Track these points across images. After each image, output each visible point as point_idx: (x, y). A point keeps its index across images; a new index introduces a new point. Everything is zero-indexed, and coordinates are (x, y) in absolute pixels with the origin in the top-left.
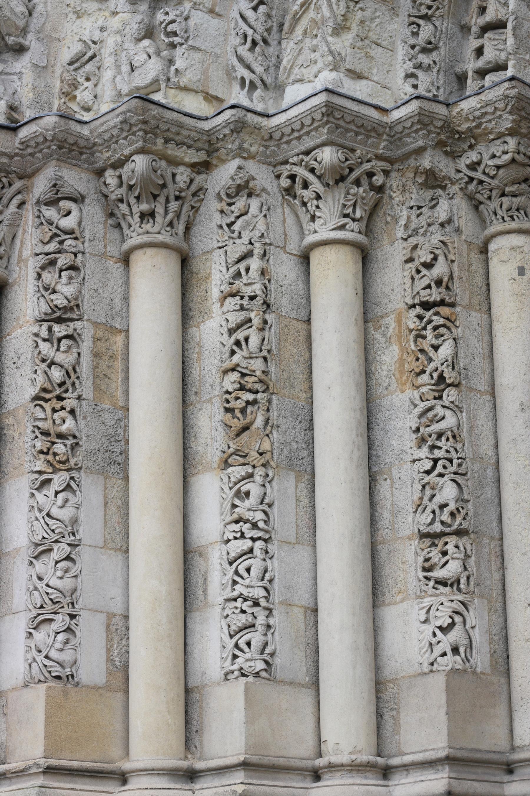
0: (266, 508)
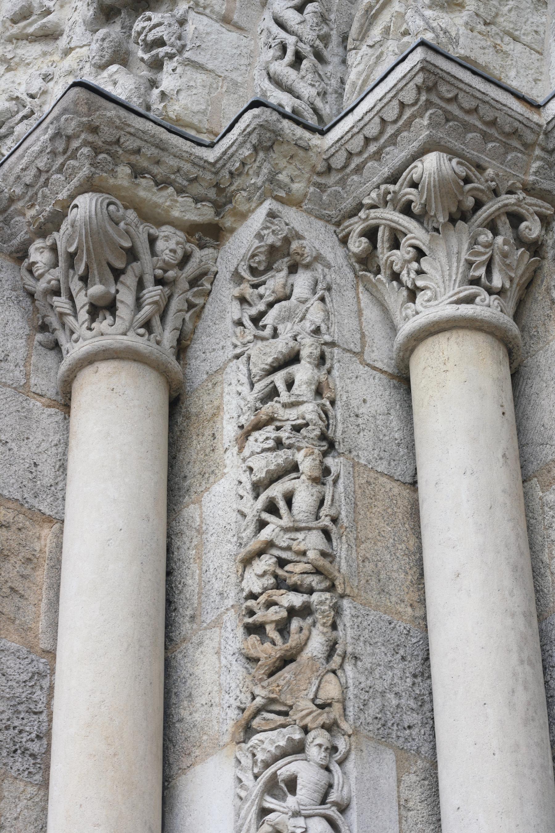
0: (333, 812)
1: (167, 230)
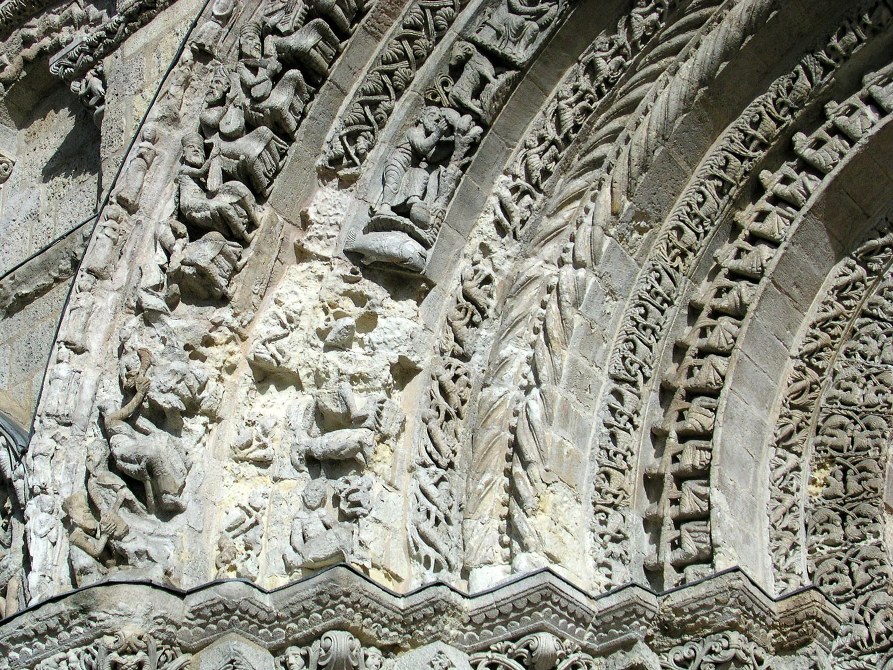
1: (372, 651)
